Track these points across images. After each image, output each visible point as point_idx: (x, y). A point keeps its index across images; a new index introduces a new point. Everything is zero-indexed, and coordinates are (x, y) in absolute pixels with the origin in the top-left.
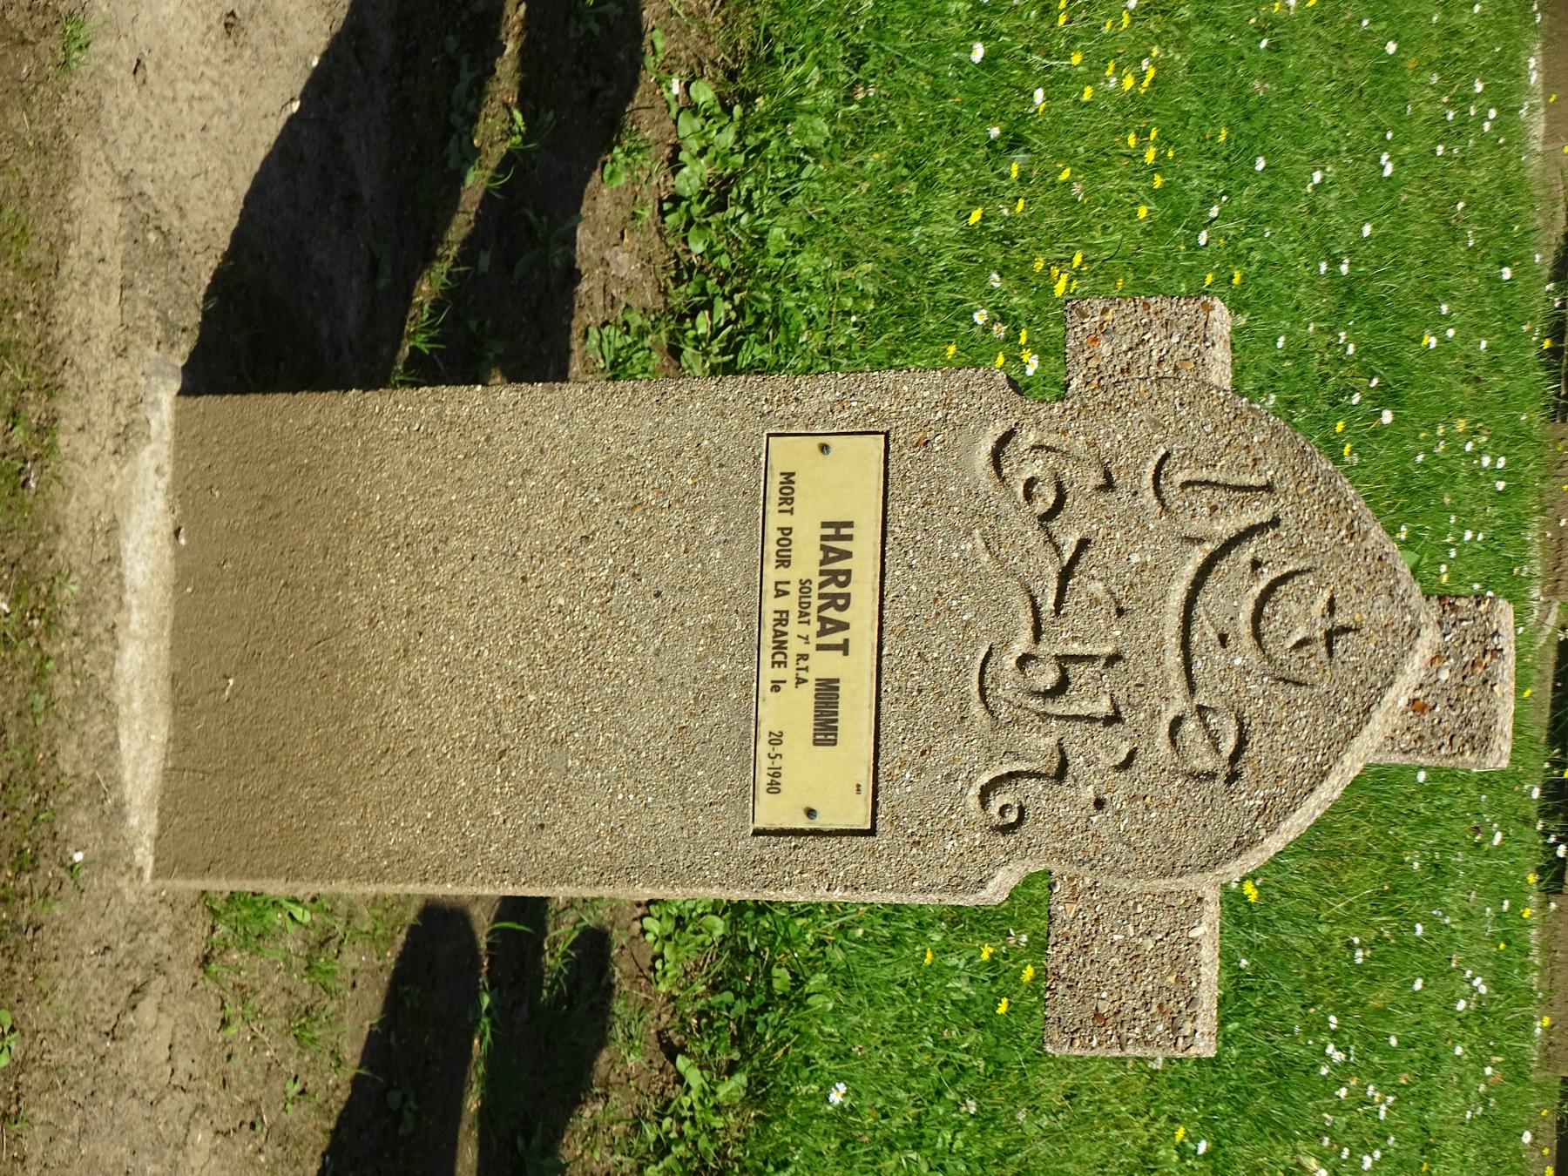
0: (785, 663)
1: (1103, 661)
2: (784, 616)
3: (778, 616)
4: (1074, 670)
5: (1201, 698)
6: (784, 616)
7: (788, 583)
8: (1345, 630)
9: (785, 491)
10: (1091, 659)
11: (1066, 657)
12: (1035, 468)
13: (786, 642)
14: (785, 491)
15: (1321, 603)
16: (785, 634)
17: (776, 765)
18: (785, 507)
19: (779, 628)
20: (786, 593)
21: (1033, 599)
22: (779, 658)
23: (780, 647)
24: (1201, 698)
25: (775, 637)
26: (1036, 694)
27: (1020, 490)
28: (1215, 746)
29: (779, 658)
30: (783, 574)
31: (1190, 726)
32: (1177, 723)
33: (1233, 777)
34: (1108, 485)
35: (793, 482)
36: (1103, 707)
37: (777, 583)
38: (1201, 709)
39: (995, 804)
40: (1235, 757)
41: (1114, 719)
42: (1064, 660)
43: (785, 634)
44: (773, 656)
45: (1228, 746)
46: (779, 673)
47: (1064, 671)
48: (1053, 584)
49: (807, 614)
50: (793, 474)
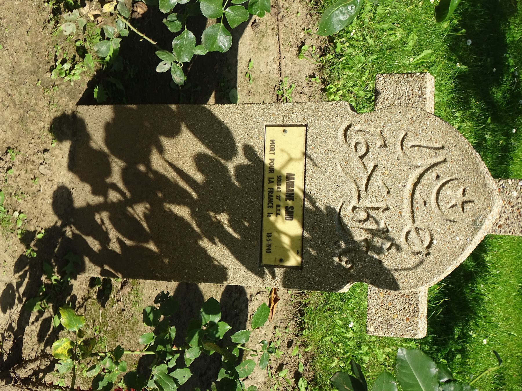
0: (272, 207)
1: (382, 210)
2: (272, 190)
3: (269, 190)
5: (417, 224)
6: (272, 190)
7: (273, 178)
9: (272, 146)
10: (379, 209)
11: (370, 208)
12: (360, 138)
13: (273, 199)
14: (272, 146)
16: (272, 196)
17: (270, 242)
18: (272, 152)
19: (270, 194)
20: (273, 182)
22: (270, 205)
23: (270, 200)
25: (268, 197)
26: (360, 221)
27: (353, 147)
28: (422, 241)
29: (270, 205)
30: (271, 175)
31: (413, 234)
32: (408, 233)
33: (428, 254)
34: (385, 146)
35: (274, 143)
37: (269, 178)
38: (416, 228)
40: (429, 246)
42: (367, 209)
43: (272, 196)
44: (268, 204)
46: (271, 210)
47: (368, 213)
48: (364, 182)
49: (280, 188)
50: (274, 140)
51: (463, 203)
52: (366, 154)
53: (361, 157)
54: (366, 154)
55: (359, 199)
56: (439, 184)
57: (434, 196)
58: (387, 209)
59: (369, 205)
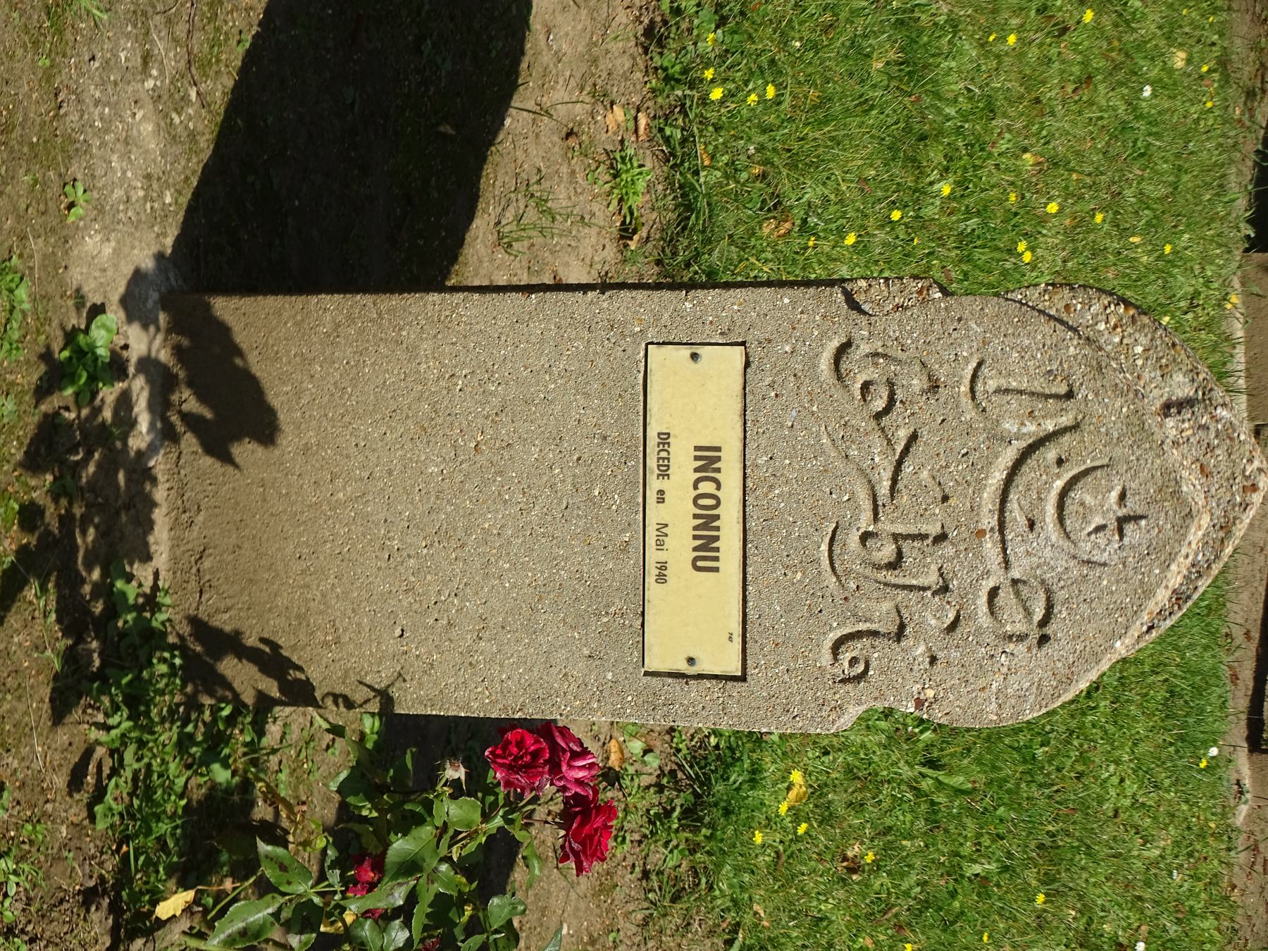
1: (929, 541)
4: (906, 546)
8: (1136, 518)
10: (923, 537)
15: (1114, 495)
21: (873, 488)
24: (1016, 573)
26: (878, 567)
28: (1028, 613)
32: (993, 593)
36: (932, 579)
38: (1015, 582)
39: (846, 657)
41: (945, 589)
42: (896, 537)
45: (1039, 613)
48: (886, 475)
51: (1122, 522)
52: (887, 410)
53: (878, 416)
54: (887, 410)
55: (876, 514)
56: (1067, 476)
57: (1050, 509)
58: (941, 538)
59: (900, 529)
